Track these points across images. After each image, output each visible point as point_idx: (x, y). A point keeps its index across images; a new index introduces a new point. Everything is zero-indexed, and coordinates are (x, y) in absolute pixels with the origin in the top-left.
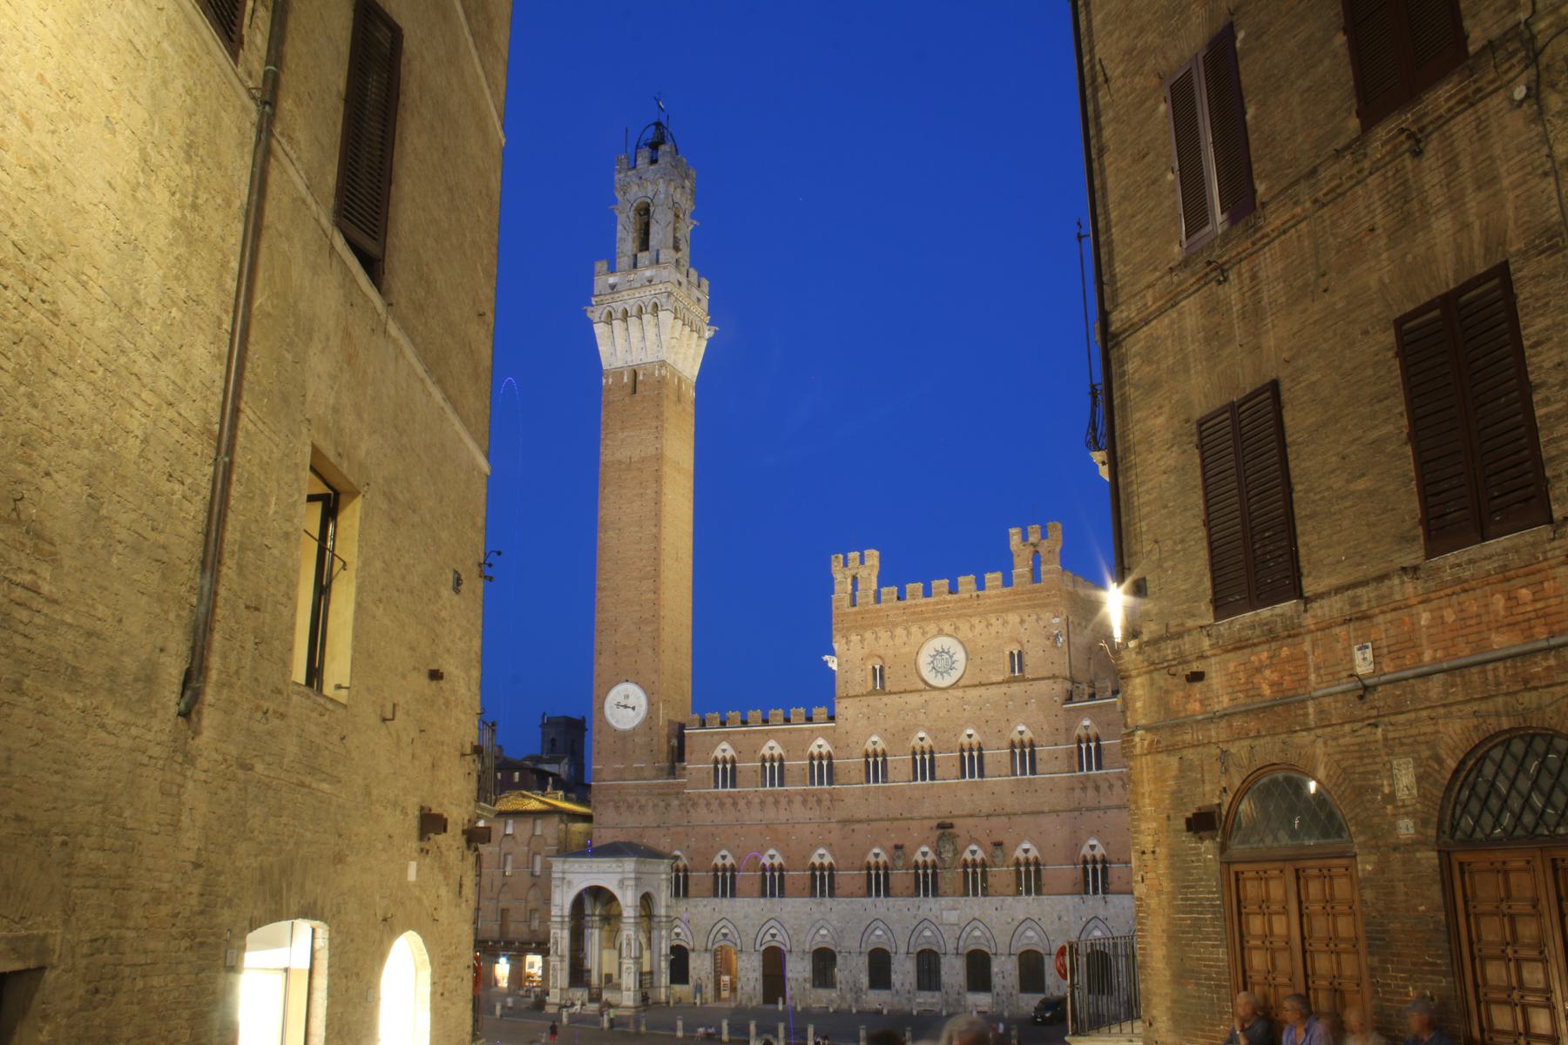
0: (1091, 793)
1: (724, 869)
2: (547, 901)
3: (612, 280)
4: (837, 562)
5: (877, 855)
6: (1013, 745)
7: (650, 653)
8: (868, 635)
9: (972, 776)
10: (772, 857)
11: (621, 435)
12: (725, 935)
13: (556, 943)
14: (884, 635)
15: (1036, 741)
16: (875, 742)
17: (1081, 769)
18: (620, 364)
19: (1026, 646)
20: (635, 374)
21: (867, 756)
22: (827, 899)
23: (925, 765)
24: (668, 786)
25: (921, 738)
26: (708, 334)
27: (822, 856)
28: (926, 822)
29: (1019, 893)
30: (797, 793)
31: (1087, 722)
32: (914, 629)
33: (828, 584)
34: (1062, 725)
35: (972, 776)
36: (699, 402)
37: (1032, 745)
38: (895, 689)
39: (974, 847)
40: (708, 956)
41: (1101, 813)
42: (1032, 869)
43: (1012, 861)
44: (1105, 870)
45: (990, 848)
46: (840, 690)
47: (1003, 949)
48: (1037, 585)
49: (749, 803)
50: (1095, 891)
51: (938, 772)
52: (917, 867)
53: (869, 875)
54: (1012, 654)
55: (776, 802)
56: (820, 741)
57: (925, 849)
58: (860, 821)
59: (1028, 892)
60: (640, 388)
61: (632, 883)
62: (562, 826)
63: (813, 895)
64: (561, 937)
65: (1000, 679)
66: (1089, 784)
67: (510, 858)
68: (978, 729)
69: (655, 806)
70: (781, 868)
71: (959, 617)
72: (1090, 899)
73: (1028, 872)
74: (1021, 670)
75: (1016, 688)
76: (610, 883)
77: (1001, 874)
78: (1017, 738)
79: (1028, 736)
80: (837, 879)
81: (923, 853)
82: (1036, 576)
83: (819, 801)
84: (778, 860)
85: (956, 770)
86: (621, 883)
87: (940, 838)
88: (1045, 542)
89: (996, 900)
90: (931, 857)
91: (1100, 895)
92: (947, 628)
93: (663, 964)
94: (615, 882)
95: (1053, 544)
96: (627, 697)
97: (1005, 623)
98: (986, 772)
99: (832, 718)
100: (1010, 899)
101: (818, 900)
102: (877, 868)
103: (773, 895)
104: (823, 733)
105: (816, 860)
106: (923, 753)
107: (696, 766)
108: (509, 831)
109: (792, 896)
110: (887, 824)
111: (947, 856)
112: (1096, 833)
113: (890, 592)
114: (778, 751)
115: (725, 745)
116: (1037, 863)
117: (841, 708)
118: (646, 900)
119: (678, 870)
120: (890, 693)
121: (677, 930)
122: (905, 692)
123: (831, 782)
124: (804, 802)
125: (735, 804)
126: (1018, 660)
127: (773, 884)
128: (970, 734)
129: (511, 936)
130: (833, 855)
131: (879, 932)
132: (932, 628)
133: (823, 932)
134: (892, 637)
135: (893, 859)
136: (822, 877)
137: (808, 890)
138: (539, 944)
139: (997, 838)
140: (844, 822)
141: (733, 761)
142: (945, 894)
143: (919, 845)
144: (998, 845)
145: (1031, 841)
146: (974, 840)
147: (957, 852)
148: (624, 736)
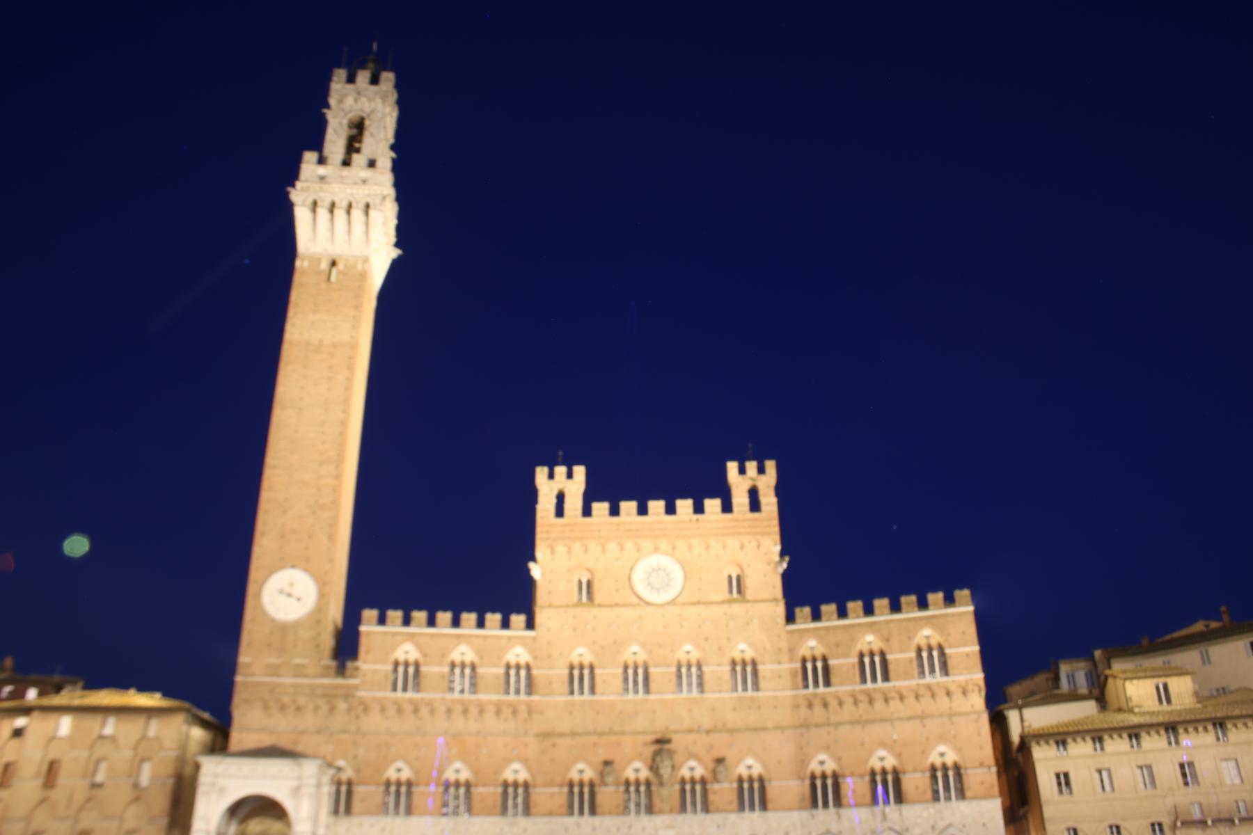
0: (818, 710)
1: (399, 784)
3: (322, 170)
4: (541, 473)
6: (734, 663)
8: (577, 547)
9: (690, 690)
14: (594, 548)
15: (758, 660)
16: (582, 654)
17: (806, 686)
19: (748, 571)
20: (334, 263)
21: (572, 668)
24: (337, 687)
25: (635, 652)
29: (741, 807)
30: (491, 703)
32: (629, 546)
33: (532, 495)
34: (784, 645)
35: (690, 690)
37: (754, 663)
41: (831, 729)
45: (711, 765)
48: (756, 515)
49: (432, 711)
50: (826, 804)
51: (653, 686)
53: (571, 792)
54: (730, 578)
55: (465, 712)
57: (638, 765)
58: (562, 735)
59: (752, 808)
62: (184, 728)
65: (720, 598)
69: (316, 709)
70: (468, 785)
71: (677, 537)
72: (820, 813)
73: (751, 789)
75: (738, 609)
77: (724, 790)
79: (749, 656)
81: (637, 770)
82: (755, 505)
83: (515, 712)
84: (465, 775)
86: (296, 791)
87: (656, 754)
88: (763, 477)
90: (644, 773)
91: (832, 809)
95: (767, 482)
96: (292, 585)
97: (724, 547)
99: (530, 625)
100: (733, 817)
101: (509, 819)
104: (521, 641)
105: (509, 775)
109: (480, 814)
110: (595, 739)
111: (665, 771)
112: (827, 749)
113: (601, 508)
114: (470, 657)
117: (541, 616)
120: (600, 606)
122: (617, 605)
123: (530, 691)
124: (498, 713)
126: (738, 585)
128: (688, 651)
130: (529, 769)
132: (647, 545)
134: (604, 550)
137: (499, 808)
139: (718, 753)
140: (545, 735)
141: (417, 665)
142: (661, 812)
145: (755, 756)
147: (674, 768)
148: (284, 629)
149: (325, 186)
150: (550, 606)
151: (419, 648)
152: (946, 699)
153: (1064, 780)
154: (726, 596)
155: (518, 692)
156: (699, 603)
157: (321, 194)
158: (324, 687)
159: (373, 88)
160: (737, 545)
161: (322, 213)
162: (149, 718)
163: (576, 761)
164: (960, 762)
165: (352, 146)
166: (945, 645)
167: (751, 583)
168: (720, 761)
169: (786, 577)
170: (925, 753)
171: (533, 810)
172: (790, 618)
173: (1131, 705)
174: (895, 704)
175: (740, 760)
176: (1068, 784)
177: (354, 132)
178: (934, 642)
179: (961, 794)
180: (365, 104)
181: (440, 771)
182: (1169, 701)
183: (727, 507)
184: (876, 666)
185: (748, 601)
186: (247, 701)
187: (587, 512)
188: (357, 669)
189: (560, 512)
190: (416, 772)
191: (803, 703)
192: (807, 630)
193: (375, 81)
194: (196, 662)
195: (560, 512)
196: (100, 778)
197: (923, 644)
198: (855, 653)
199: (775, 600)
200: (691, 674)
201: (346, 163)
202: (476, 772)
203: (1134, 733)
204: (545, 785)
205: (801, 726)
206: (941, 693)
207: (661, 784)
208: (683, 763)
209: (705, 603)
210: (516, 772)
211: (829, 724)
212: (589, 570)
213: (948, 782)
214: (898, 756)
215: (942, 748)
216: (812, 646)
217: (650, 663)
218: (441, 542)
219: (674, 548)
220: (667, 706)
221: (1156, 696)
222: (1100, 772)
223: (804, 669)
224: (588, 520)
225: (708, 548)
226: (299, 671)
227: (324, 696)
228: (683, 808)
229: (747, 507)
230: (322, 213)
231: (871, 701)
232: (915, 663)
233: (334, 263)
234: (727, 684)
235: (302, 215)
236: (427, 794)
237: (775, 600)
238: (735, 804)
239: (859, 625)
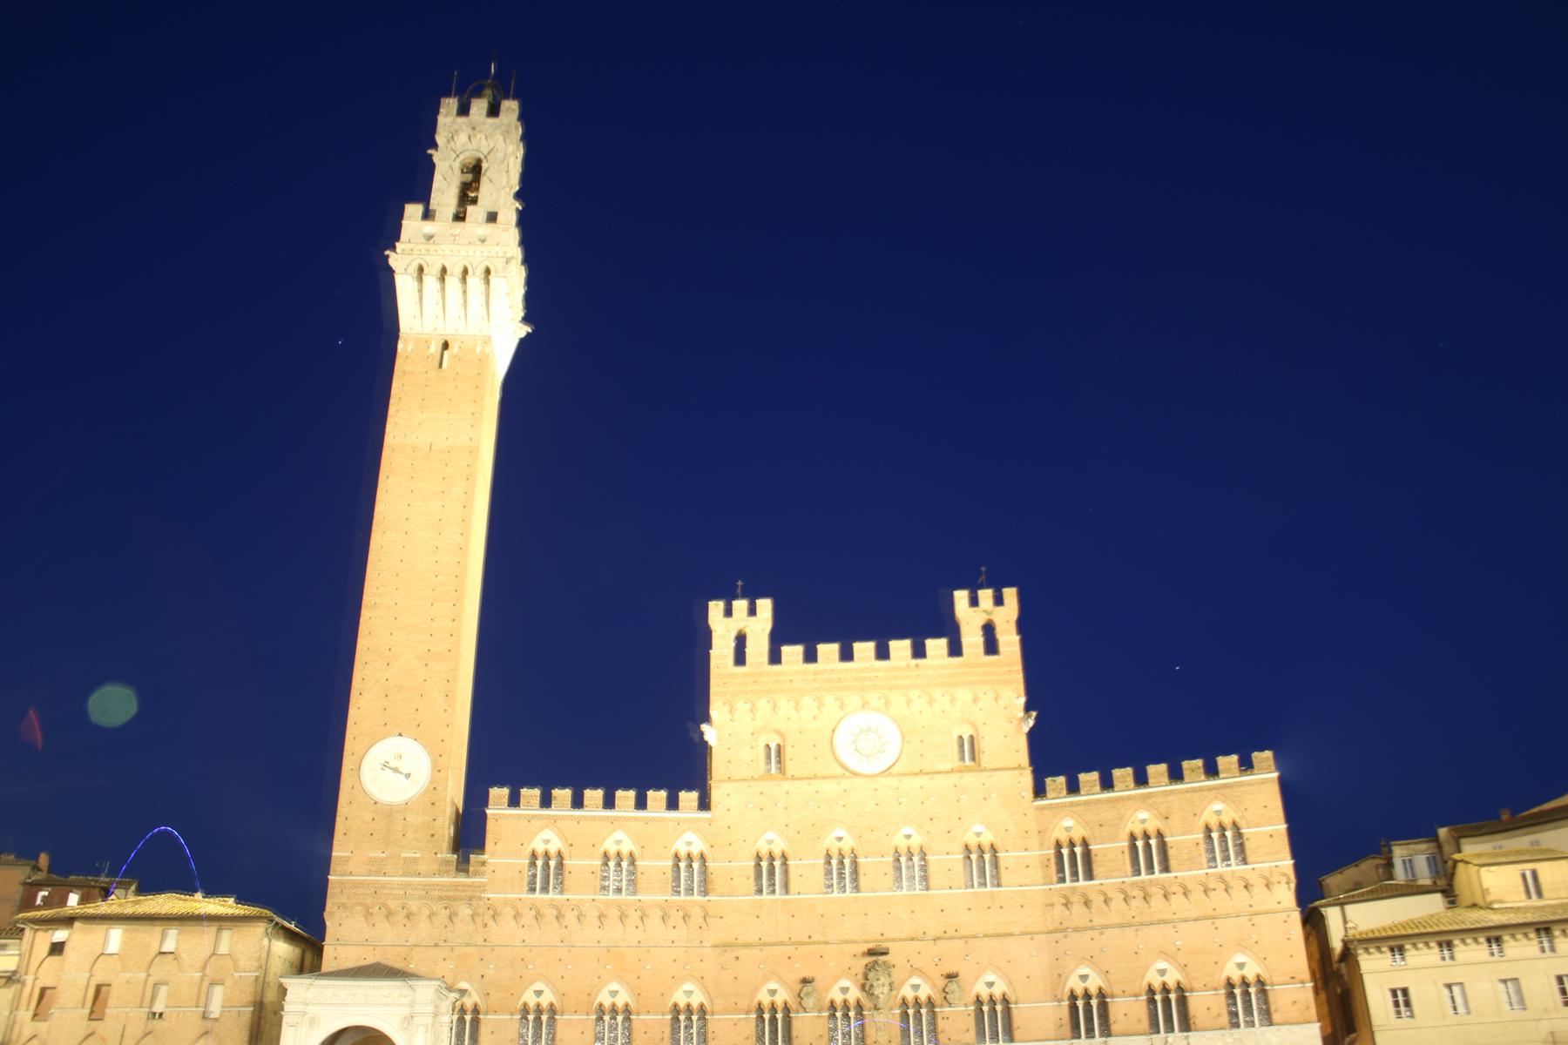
0: (1078, 908)
3: (428, 227)
4: (716, 608)
5: (773, 992)
6: (967, 848)
8: (763, 704)
10: (614, 993)
14: (785, 705)
15: (999, 846)
17: (1063, 880)
20: (446, 346)
21: (759, 858)
23: (844, 870)
24: (457, 887)
25: (837, 838)
26: (524, 330)
27: (689, 993)
28: (846, 946)
31: (1068, 822)
32: (830, 700)
33: (704, 637)
37: (994, 849)
38: (797, 774)
39: (916, 980)
41: (1095, 934)
43: (972, 998)
44: (1103, 1006)
46: (719, 766)
51: (863, 881)
53: (761, 1018)
55: (623, 917)
58: (747, 946)
61: (429, 1020)
65: (948, 767)
66: (1075, 899)
67: (163, 990)
70: (627, 1011)
71: (892, 688)
73: (993, 1011)
74: (973, 758)
75: (970, 779)
78: (973, 842)
80: (711, 1027)
82: (991, 646)
87: (869, 968)
90: (854, 994)
95: (1006, 615)
97: (953, 700)
98: (932, 882)
99: (704, 804)
108: (169, 946)
110: (789, 950)
111: (881, 990)
115: (548, 834)
117: (717, 793)
119: (463, 1011)
122: (815, 777)
123: (705, 893)
126: (970, 749)
128: (908, 835)
132: (853, 700)
140: (727, 946)
143: (838, 978)
148: (390, 813)
149: (432, 248)
151: (563, 836)
152: (1244, 892)
153: (1402, 999)
154: (956, 763)
155: (690, 891)
157: (427, 258)
158: (442, 887)
159: (491, 121)
160: (968, 696)
161: (431, 281)
162: (220, 930)
163: (767, 979)
164: (1265, 976)
165: (467, 194)
166: (1241, 824)
167: (987, 746)
168: (951, 977)
169: (1032, 736)
172: (1040, 791)
173: (1489, 898)
174: (1177, 900)
176: (1407, 1004)
177: (469, 177)
178: (1227, 821)
179: (1268, 1019)
180: (481, 142)
182: (1540, 894)
183: (955, 649)
184: (1151, 852)
185: (985, 770)
186: (344, 906)
187: (775, 658)
188: (483, 864)
189: (740, 658)
191: (1059, 901)
192: (1062, 806)
193: (494, 111)
194: (276, 859)
195: (740, 658)
196: (158, 1008)
198: (1125, 835)
199: (1019, 767)
201: (460, 217)
203: (1494, 936)
204: (727, 1012)
205: (1056, 931)
206: (1237, 885)
207: (876, 1008)
208: (903, 982)
210: (688, 994)
211: (1092, 928)
212: (779, 733)
213: (1249, 1000)
217: (859, 852)
218: (588, 700)
219: (887, 703)
220: (880, 910)
221: (1521, 888)
222: (1449, 986)
223: (1059, 856)
224: (776, 668)
225: (931, 702)
226: (410, 868)
227: (441, 898)
229: (981, 649)
230: (431, 281)
232: (1203, 847)
233: (446, 346)
235: (405, 286)
237: (1019, 767)
239: (1129, 798)
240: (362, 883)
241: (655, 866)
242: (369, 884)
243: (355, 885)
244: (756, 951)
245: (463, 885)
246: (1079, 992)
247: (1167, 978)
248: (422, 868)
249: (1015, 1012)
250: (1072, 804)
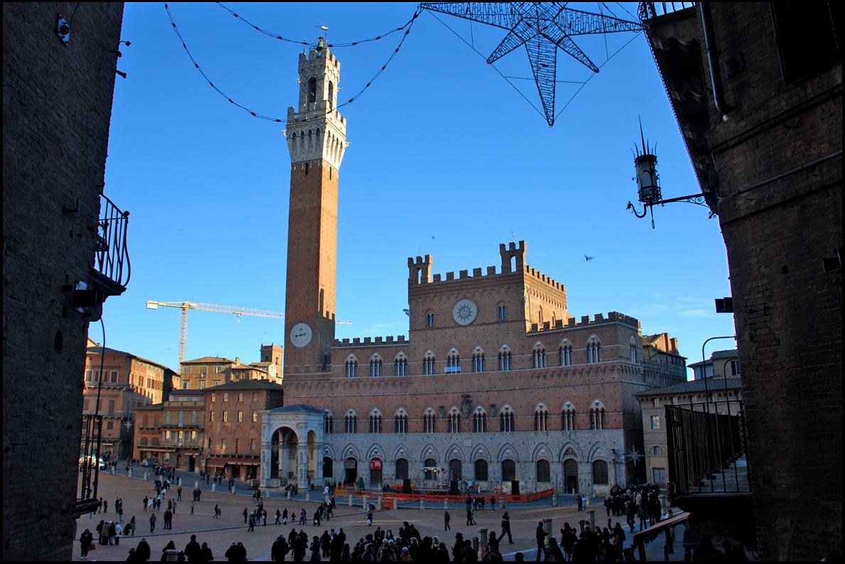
0: (541, 379)
1: (351, 418)
2: (260, 434)
5: (430, 411)
6: (500, 355)
7: (314, 307)
10: (376, 412)
11: (300, 196)
12: (351, 452)
13: (264, 456)
16: (430, 353)
18: (301, 160)
20: (307, 165)
21: (425, 360)
22: (404, 433)
24: (323, 376)
27: (401, 412)
29: (502, 430)
31: (538, 343)
36: (340, 180)
39: (480, 407)
40: (343, 463)
42: (510, 418)
43: (499, 415)
47: (494, 459)
52: (450, 416)
53: (425, 421)
55: (379, 385)
56: (401, 353)
57: (454, 408)
59: (507, 430)
60: (309, 172)
63: (397, 431)
64: (266, 454)
65: (494, 320)
68: (482, 346)
69: (317, 386)
70: (380, 418)
73: (507, 419)
75: (502, 325)
76: (291, 425)
78: (502, 351)
79: (508, 350)
80: (409, 423)
81: (454, 410)
85: (470, 368)
86: (297, 426)
89: (491, 434)
92: (468, 295)
93: (321, 467)
94: (295, 425)
96: (301, 330)
100: (498, 433)
102: (430, 417)
103: (376, 431)
106: (453, 358)
107: (337, 366)
109: (385, 432)
110: (435, 396)
112: (543, 399)
115: (351, 355)
116: (512, 414)
118: (311, 434)
119: (327, 419)
120: (437, 328)
121: (327, 450)
122: (445, 328)
125: (358, 385)
127: (375, 425)
128: (479, 350)
129: (240, 453)
130: (407, 411)
131: (430, 451)
133: (402, 450)
135: (438, 414)
136: (401, 421)
138: (255, 457)
139: (491, 402)
140: (415, 395)
142: (464, 431)
143: (451, 406)
144: (493, 406)
145: (509, 404)
146: (479, 403)
147: (471, 410)
150: (416, 330)
151: (357, 357)
156: (484, 324)
163: (427, 406)
164: (605, 408)
170: (589, 403)
171: (409, 430)
175: (502, 405)
178: (596, 342)
181: (368, 413)
185: (508, 322)
188: (330, 367)
190: (358, 413)
197: (591, 342)
198: (558, 348)
200: (478, 360)
202: (384, 412)
204: (415, 418)
209: (486, 324)
210: (401, 412)
214: (576, 404)
215: (596, 401)
216: (538, 344)
228: (475, 431)
231: (566, 375)
232: (586, 354)
233: (307, 165)
234: (496, 368)
236: (363, 424)
238: (498, 429)
240: (294, 376)
241: (388, 364)
242: (296, 376)
243: (291, 376)
244: (424, 396)
245: (323, 375)
246: (539, 412)
247: (570, 408)
248: (311, 370)
249: (515, 420)
250: (540, 335)
